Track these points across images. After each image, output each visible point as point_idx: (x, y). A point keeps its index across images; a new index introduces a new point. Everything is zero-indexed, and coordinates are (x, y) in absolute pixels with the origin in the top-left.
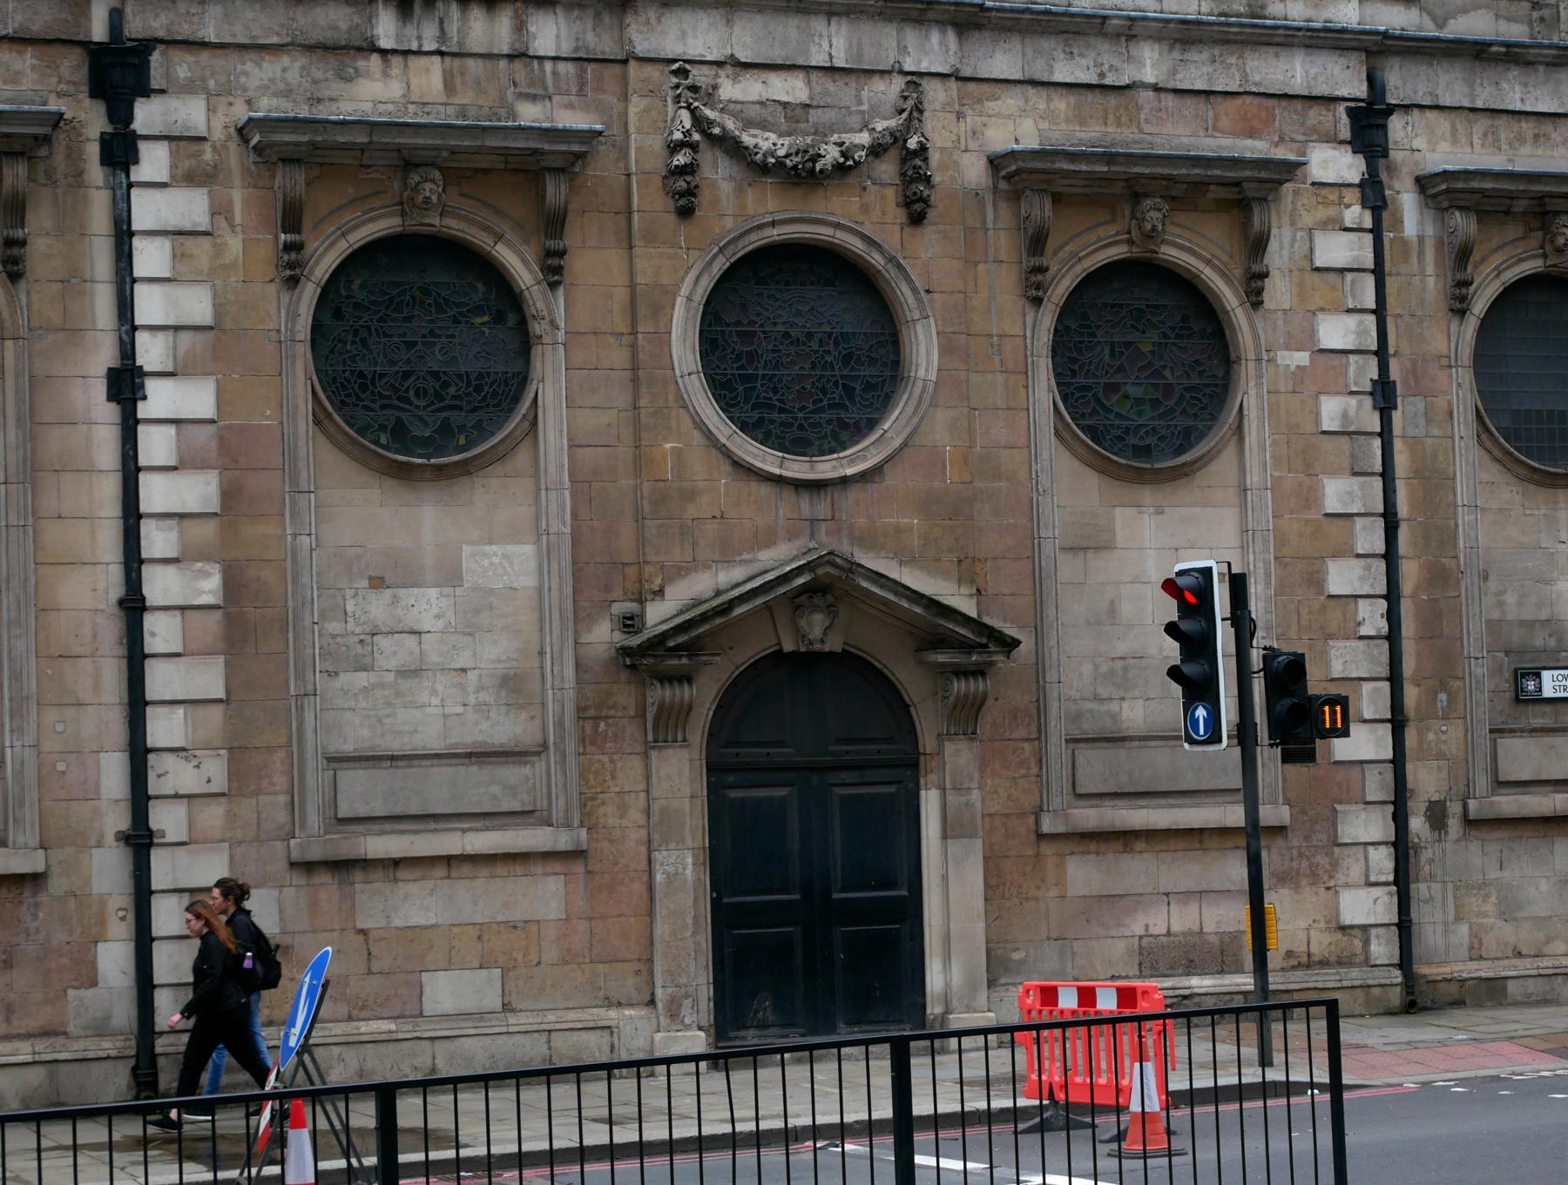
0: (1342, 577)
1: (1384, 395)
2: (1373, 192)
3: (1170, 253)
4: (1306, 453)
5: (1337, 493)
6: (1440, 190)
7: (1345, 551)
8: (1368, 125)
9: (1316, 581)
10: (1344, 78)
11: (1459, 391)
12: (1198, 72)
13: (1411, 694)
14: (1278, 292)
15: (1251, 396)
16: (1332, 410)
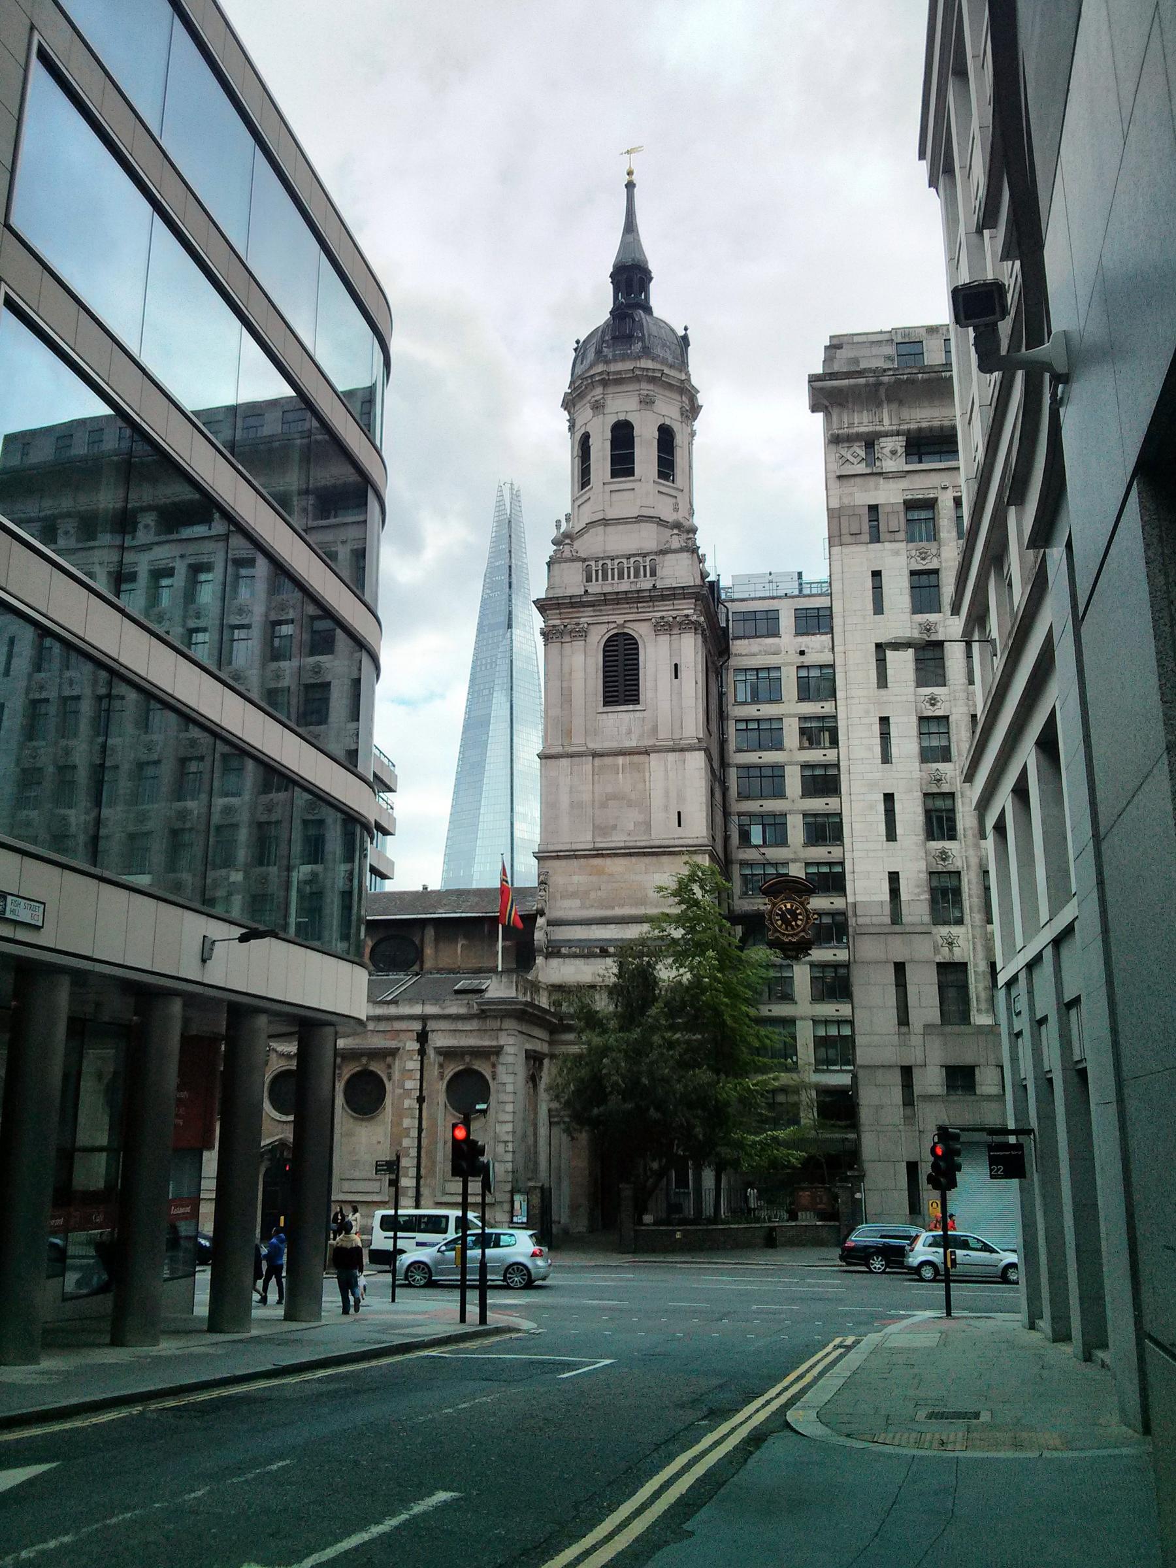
0: (406, 1142)
1: (421, 1100)
2: (422, 1052)
3: (371, 1068)
4: (399, 1114)
5: (407, 1122)
6: (440, 1051)
7: (408, 1136)
8: (422, 1037)
9: (400, 1144)
10: (417, 1026)
11: (442, 1098)
12: (382, 1026)
13: (423, 1172)
14: (396, 1076)
15: (388, 1100)
16: (407, 1103)
